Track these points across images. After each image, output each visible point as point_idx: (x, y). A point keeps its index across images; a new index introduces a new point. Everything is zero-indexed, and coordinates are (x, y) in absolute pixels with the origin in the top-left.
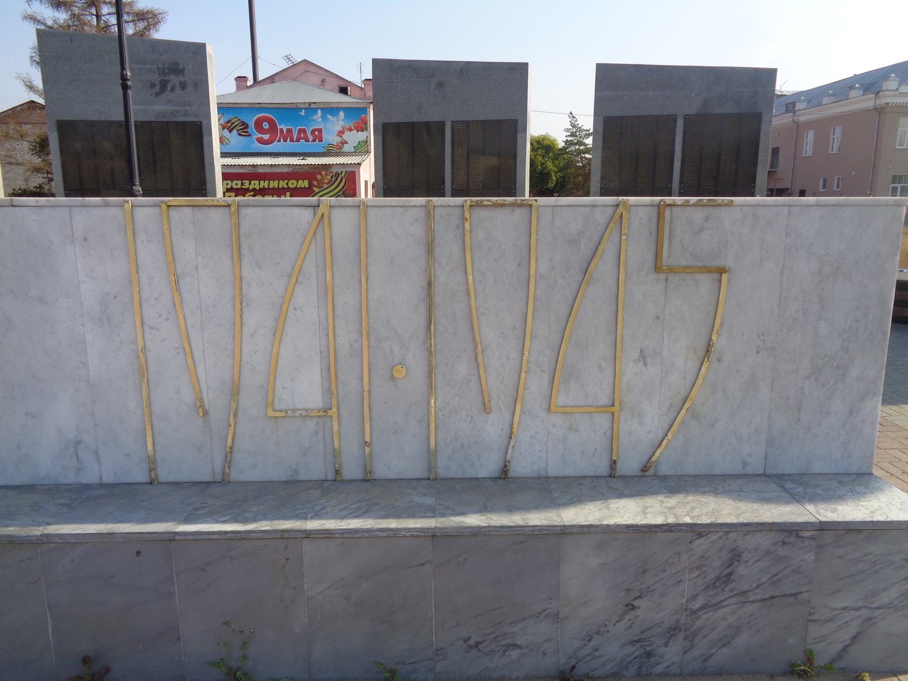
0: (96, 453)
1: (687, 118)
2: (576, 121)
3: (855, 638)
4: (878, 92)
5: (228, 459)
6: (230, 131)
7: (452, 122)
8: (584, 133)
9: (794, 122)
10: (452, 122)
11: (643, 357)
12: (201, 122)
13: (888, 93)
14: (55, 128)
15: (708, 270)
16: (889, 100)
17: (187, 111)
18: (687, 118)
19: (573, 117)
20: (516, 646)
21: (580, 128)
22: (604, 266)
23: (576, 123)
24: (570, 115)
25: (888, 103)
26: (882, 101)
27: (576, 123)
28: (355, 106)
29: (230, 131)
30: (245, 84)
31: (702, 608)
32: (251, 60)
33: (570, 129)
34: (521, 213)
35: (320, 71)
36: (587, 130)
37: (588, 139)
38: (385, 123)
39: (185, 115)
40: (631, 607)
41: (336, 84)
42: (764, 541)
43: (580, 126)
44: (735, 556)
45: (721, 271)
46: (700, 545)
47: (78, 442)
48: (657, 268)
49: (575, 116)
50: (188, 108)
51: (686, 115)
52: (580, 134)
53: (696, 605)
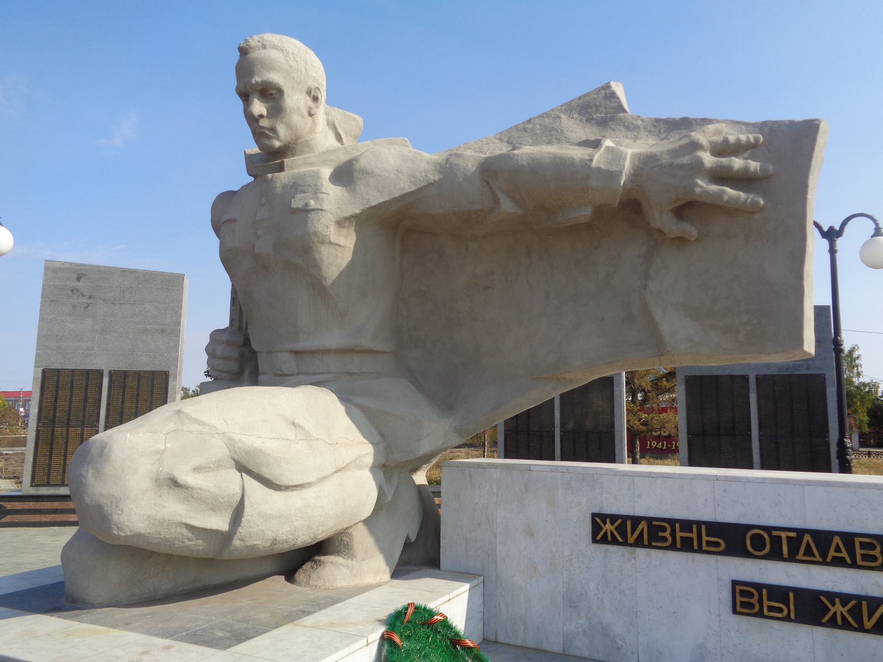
12: (825, 374)
14: (683, 382)
17: (810, 365)
39: (808, 369)
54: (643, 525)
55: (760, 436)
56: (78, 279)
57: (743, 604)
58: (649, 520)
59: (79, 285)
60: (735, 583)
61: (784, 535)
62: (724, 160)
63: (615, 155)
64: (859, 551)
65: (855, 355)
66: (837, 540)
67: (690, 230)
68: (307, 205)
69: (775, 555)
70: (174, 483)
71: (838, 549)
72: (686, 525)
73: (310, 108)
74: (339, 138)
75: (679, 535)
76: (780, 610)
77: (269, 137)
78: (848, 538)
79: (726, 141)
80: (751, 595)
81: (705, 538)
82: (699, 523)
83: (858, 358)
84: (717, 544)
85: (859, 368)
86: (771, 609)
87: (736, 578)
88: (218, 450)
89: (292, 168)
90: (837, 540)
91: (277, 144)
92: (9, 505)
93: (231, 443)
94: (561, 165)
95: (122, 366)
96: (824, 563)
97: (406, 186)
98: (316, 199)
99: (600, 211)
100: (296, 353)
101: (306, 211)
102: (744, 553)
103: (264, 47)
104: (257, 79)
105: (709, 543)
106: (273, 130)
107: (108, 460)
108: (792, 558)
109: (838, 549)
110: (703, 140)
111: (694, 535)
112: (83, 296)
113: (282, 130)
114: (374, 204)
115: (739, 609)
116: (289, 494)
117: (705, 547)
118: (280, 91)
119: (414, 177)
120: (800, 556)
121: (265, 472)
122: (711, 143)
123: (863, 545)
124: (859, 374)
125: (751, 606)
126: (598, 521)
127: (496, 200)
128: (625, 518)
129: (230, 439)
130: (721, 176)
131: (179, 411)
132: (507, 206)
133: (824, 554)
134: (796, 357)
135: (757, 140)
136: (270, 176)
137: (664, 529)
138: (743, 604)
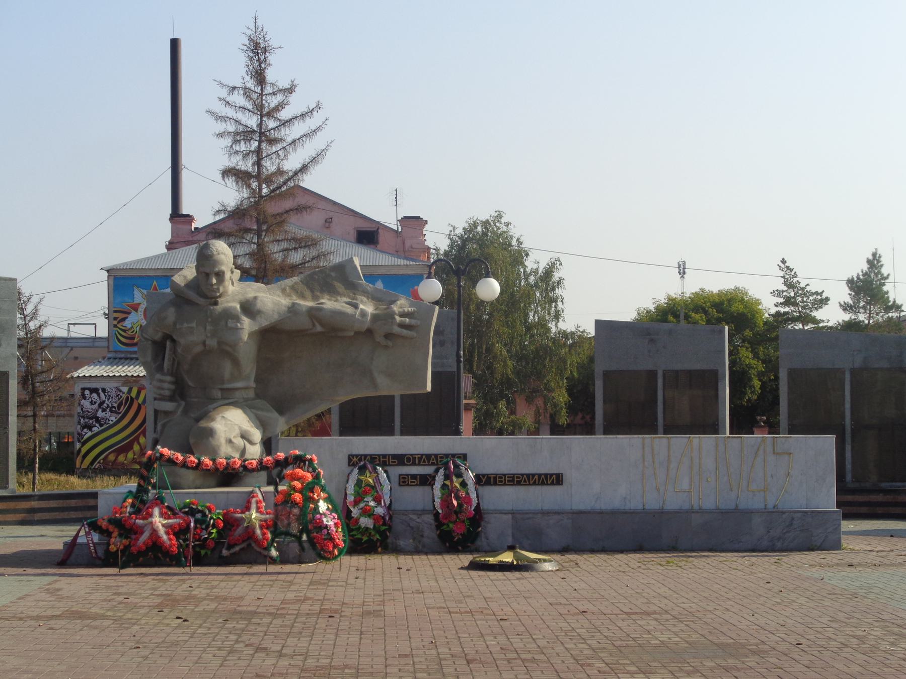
0: (630, 501)
1: (853, 372)
3: (823, 541)
5: (664, 504)
7: (664, 371)
8: (811, 298)
10: (664, 371)
11: (772, 476)
15: (787, 454)
18: (853, 372)
19: (788, 268)
20: (741, 542)
21: (803, 289)
22: (761, 452)
23: (795, 280)
24: (782, 266)
27: (795, 280)
28: (401, 272)
30: (186, 227)
31: (787, 532)
32: (169, 172)
33: (783, 292)
34: (739, 440)
35: (322, 205)
36: (817, 293)
37: (820, 310)
38: (606, 371)
40: (769, 532)
41: (350, 227)
42: (799, 515)
43: (802, 285)
44: (793, 519)
45: (790, 454)
46: (784, 516)
47: (625, 498)
48: (774, 453)
49: (791, 267)
50: (445, 361)
51: (851, 369)
52: (803, 301)
53: (785, 531)
54: (369, 457)
55: (402, 427)
57: (403, 482)
58: (371, 455)
60: (400, 475)
61: (417, 456)
62: (403, 319)
63: (363, 314)
64: (439, 460)
65: (556, 276)
66: (433, 456)
67: (390, 343)
68: (237, 326)
69: (414, 464)
70: (230, 441)
71: (433, 460)
72: (384, 456)
73: (231, 277)
74: (233, 284)
75: (382, 460)
76: (414, 482)
77: (216, 292)
78: (436, 455)
79: (404, 310)
80: (405, 478)
81: (391, 460)
82: (389, 455)
83: (559, 283)
84: (395, 462)
85: (560, 304)
86: (412, 482)
87: (400, 473)
88: (237, 431)
89: (221, 304)
90: (433, 456)
91: (218, 294)
93: (240, 428)
96: (429, 465)
97: (276, 317)
98: (240, 323)
99: (357, 333)
100: (222, 389)
101: (237, 329)
102: (404, 464)
103: (219, 254)
104: (217, 269)
105: (392, 462)
106: (218, 289)
107: (216, 433)
108: (419, 464)
109: (433, 460)
110: (395, 308)
111: (387, 460)
113: (221, 289)
114: (263, 325)
115: (401, 484)
116: (254, 446)
117: (391, 463)
118: (223, 273)
119: (280, 313)
120: (421, 463)
121: (251, 438)
122: (399, 312)
123: (441, 457)
124: (557, 316)
125: (405, 482)
126: (351, 457)
127: (314, 325)
128: (362, 455)
129: (240, 427)
130: (402, 326)
131: (223, 417)
132: (319, 328)
133: (429, 462)
134: (425, 392)
135: (414, 310)
136: (212, 308)
137: (376, 458)
138: (403, 482)
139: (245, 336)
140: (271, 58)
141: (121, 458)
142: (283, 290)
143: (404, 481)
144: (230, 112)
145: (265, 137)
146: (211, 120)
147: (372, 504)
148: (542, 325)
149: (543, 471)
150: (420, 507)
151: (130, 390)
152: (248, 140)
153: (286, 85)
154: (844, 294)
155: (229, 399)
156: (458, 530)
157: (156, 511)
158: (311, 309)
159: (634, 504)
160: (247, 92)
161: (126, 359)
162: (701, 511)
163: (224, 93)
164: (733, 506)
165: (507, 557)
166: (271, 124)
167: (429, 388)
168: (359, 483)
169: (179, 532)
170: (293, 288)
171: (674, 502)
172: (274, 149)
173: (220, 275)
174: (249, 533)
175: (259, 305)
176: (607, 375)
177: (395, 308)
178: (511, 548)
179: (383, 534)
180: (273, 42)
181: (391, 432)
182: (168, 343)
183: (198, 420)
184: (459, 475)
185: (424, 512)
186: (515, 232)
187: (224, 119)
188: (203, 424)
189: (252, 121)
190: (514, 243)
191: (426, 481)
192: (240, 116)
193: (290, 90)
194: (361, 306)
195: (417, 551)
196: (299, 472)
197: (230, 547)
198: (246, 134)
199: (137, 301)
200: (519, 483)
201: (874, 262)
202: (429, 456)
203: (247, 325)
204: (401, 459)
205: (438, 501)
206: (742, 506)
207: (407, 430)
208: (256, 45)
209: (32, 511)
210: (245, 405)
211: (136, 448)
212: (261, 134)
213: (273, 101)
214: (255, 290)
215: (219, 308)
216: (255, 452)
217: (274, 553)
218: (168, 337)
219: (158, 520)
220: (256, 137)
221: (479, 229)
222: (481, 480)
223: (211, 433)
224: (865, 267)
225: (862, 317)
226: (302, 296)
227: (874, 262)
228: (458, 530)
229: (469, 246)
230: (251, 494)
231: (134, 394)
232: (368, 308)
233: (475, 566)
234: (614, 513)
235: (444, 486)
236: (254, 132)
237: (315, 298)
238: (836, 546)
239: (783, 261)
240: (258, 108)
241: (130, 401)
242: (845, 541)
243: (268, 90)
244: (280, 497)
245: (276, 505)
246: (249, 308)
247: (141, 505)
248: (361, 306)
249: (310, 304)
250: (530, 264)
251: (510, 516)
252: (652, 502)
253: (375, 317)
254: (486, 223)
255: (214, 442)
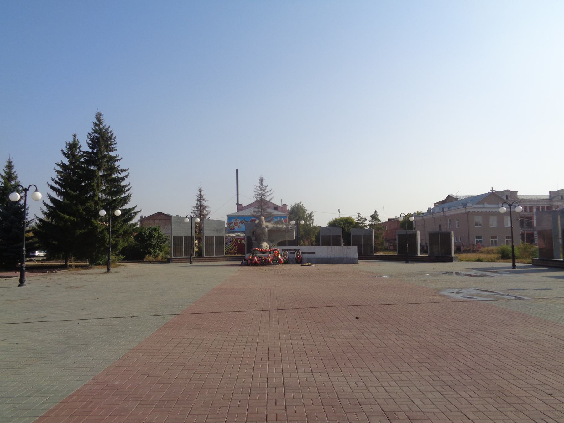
1: (363, 235)
2: (360, 215)
4: (466, 207)
6: (242, 224)
9: (444, 215)
13: (468, 208)
16: (469, 210)
25: (469, 211)
26: (467, 210)
29: (242, 224)
43: (362, 217)
56: (178, 219)
59: (178, 220)
63: (284, 227)
65: (312, 215)
70: (265, 247)
83: (313, 216)
92: (173, 259)
94: (280, 227)
95: (186, 235)
97: (271, 228)
110: (289, 227)
112: (179, 222)
126: (282, 250)
130: (290, 229)
132: (277, 230)
139: (266, 231)
140: (264, 181)
141: (231, 251)
142: (272, 224)
143: (290, 253)
144: (257, 191)
145: (262, 195)
146: (253, 192)
147: (286, 257)
148: (310, 224)
149: (312, 252)
150: (293, 257)
151: (232, 239)
152: (260, 195)
153: (266, 186)
154: (370, 219)
155: (264, 241)
156: (299, 261)
157: (256, 257)
158: (276, 227)
159: (326, 257)
160: (259, 187)
161: (231, 232)
162: (336, 258)
163: (255, 187)
164: (341, 257)
165: (307, 264)
166: (264, 193)
167: (294, 239)
168: (284, 253)
169: (259, 260)
170: (273, 223)
171: (332, 256)
172: (264, 197)
173: (263, 222)
174: (268, 261)
175: (268, 226)
176: (322, 236)
177: (289, 227)
178: (308, 263)
179: (288, 262)
180: (264, 179)
181: (286, 246)
182: (254, 232)
183: (260, 244)
184: (299, 252)
185: (293, 258)
186: (304, 206)
187: (256, 192)
188: (261, 244)
189: (260, 192)
190: (304, 208)
191: (294, 253)
192: (258, 191)
193: (267, 186)
194: (284, 226)
195: (293, 264)
196: (276, 251)
197: (266, 263)
198: (259, 194)
199: (233, 221)
200: (308, 254)
201: (376, 212)
202: (294, 249)
203: (267, 229)
204: (290, 250)
205: (296, 256)
206: (343, 257)
207: (288, 245)
208: (261, 179)
209: (228, 259)
210: (267, 242)
211: (234, 249)
212: (262, 194)
213: (264, 188)
214: (268, 224)
215: (262, 227)
216: (268, 248)
217: (272, 264)
218: (254, 231)
219: (256, 259)
220: (261, 195)
221: (297, 205)
222: (303, 253)
223: (262, 246)
224: (374, 213)
225: (373, 223)
226: (275, 225)
227: (376, 212)
228: (299, 261)
229: (295, 209)
230: (268, 255)
231: (233, 239)
232: (285, 227)
233: (302, 265)
234: (323, 258)
235: (297, 254)
236: (260, 194)
237: (276, 225)
238: (357, 263)
239: (358, 212)
240: (262, 190)
241: (232, 241)
242: (359, 263)
243: (263, 187)
244: (273, 255)
245: (273, 257)
246: (267, 227)
247: (253, 257)
248: (284, 226)
249: (276, 226)
250: (307, 212)
251: (307, 259)
252: (329, 256)
253: (286, 228)
254: (298, 204)
255: (262, 247)
